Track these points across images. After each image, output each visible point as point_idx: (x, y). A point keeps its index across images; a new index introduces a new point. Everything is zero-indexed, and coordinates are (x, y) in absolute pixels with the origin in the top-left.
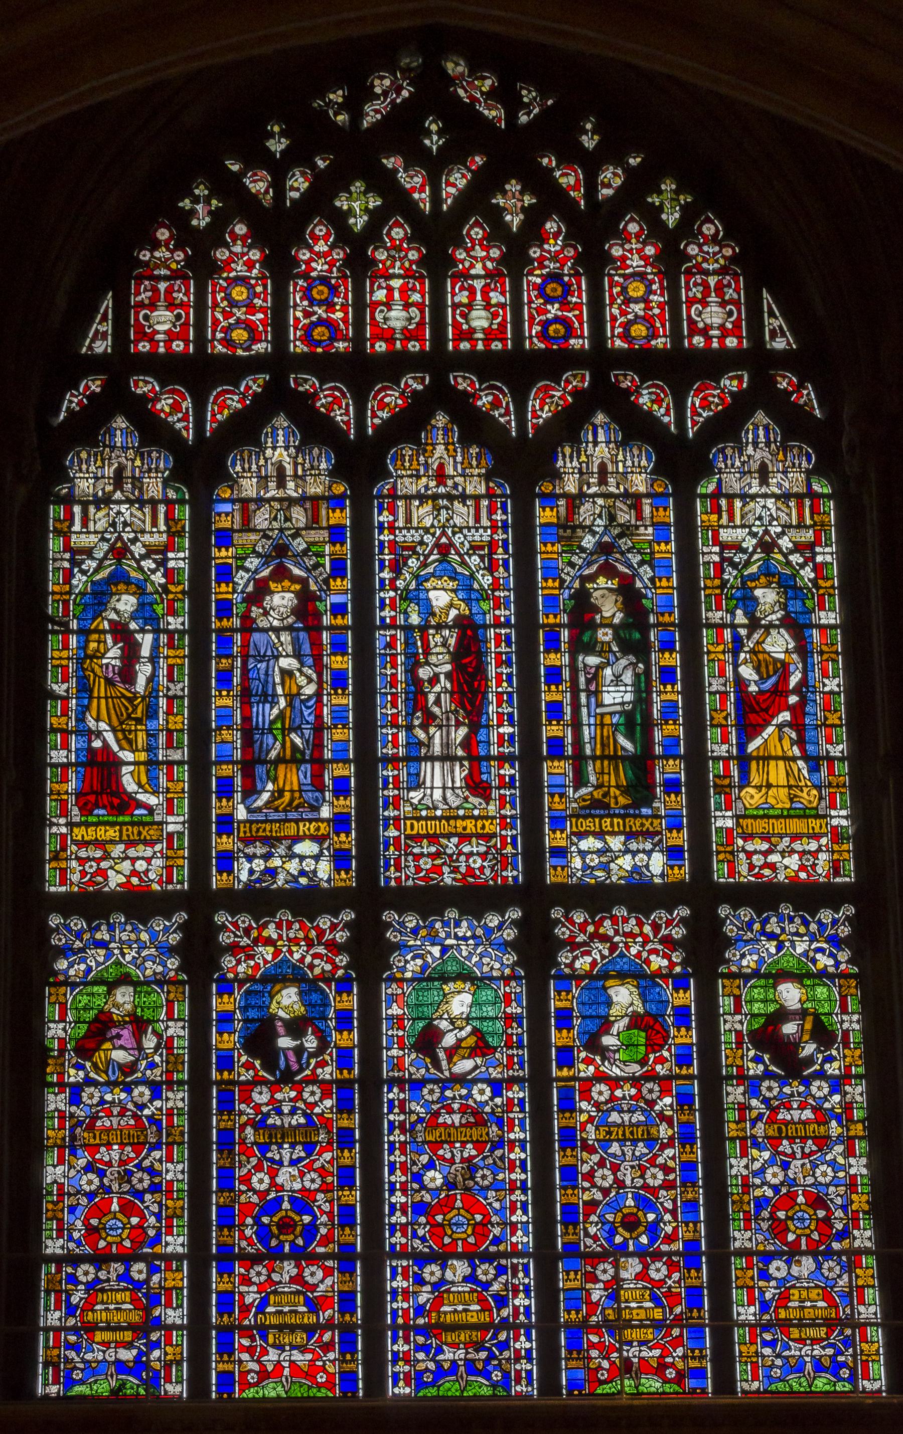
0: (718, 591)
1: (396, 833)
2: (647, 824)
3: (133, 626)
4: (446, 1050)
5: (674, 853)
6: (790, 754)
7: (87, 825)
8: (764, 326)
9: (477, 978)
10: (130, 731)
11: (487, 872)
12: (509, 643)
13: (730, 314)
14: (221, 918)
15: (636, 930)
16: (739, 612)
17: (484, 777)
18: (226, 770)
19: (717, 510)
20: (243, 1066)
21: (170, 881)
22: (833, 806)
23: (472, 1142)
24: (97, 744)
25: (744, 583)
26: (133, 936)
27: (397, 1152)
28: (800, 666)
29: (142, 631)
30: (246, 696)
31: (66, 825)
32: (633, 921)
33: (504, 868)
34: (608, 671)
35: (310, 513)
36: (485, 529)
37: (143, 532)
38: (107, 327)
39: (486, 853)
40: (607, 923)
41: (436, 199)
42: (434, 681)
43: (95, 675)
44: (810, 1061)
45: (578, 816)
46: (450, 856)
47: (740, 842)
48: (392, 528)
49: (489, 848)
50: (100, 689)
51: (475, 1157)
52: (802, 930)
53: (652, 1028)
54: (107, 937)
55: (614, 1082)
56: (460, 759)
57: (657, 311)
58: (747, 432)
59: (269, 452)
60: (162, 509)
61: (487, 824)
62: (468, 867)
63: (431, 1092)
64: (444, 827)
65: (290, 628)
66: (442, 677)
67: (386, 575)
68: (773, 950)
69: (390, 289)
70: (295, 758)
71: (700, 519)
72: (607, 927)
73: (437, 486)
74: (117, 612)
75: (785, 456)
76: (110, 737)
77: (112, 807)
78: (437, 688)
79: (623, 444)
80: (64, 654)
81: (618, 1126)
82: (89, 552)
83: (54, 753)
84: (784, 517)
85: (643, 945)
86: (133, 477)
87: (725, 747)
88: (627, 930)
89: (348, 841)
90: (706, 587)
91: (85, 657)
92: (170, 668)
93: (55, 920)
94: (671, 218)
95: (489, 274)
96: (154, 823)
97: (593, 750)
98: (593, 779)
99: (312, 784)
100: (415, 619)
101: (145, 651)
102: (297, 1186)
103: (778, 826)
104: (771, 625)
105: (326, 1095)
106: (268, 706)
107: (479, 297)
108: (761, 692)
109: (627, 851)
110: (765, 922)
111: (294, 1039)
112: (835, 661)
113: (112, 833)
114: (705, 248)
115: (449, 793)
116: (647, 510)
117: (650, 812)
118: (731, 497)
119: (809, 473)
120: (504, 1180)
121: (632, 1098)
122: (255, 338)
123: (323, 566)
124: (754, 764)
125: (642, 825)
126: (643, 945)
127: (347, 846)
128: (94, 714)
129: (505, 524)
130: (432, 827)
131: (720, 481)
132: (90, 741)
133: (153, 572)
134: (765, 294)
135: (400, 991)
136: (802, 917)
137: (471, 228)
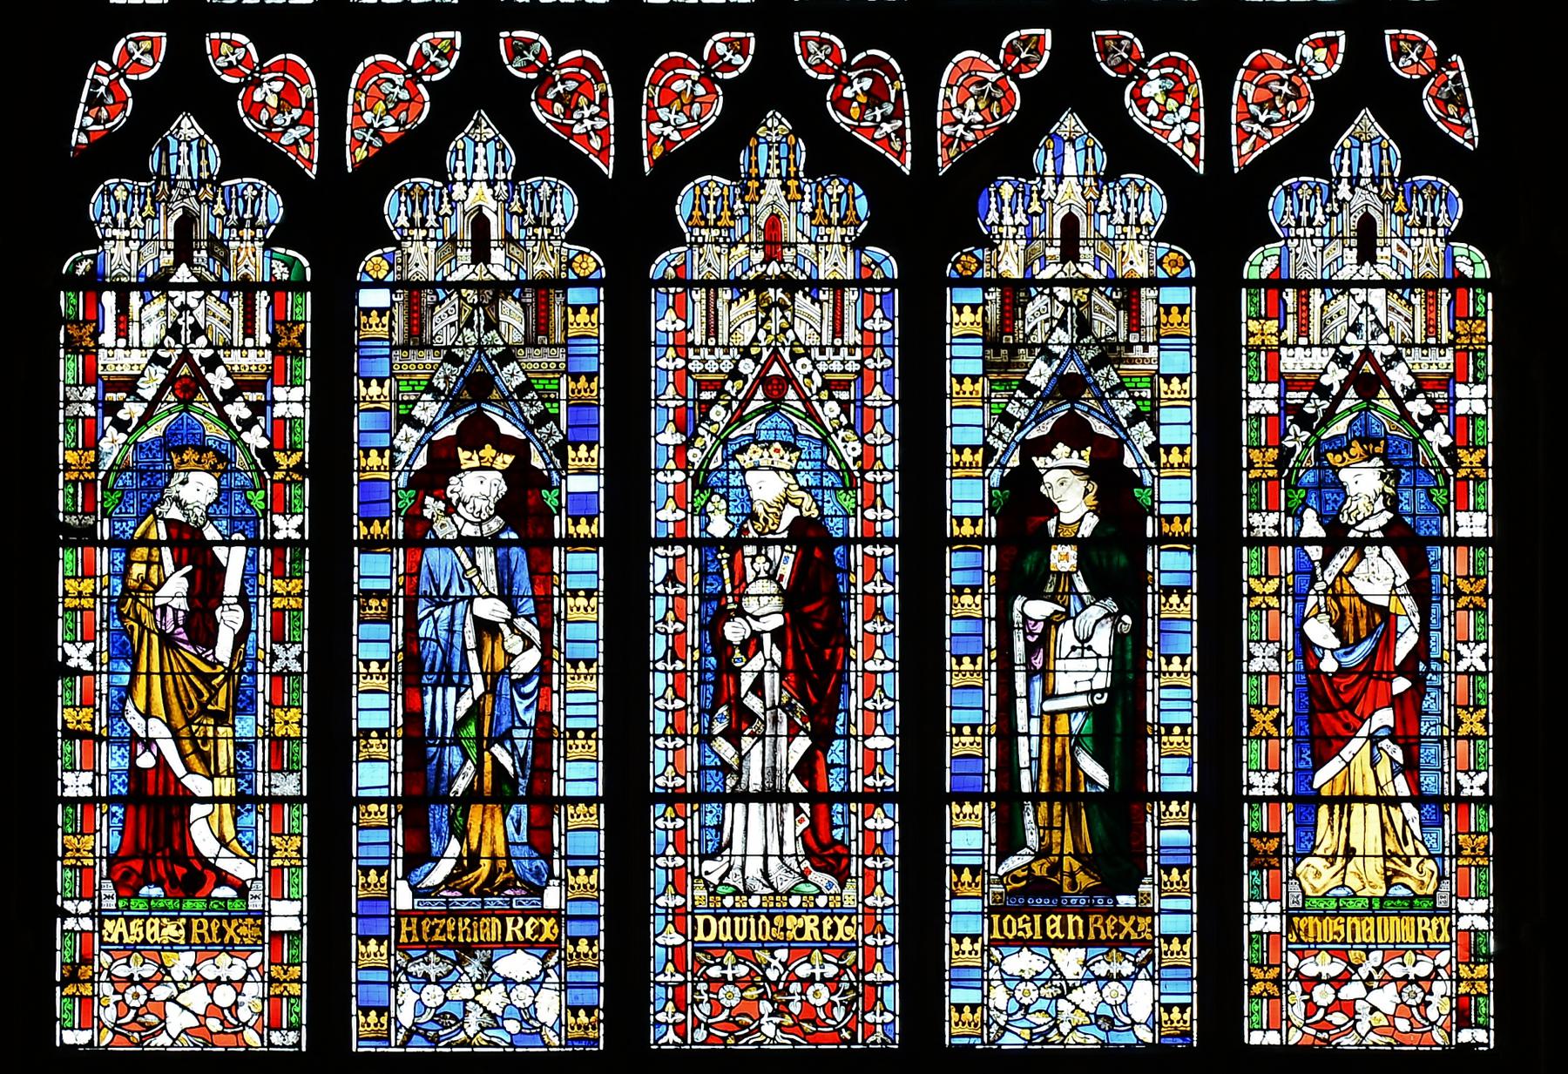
1: (679, 940)
3: (210, 533)
10: (205, 739)
16: (1310, 516)
17: (837, 834)
24: (146, 761)
25: (1320, 456)
28: (1416, 620)
29: (230, 544)
31: (91, 915)
34: (1066, 631)
35: (531, 311)
36: (852, 348)
37: (229, 346)
39: (836, 979)
42: (752, 644)
43: (142, 625)
45: (1002, 911)
47: (1293, 960)
48: (683, 346)
49: (842, 968)
50: (153, 657)
56: (796, 799)
59: (459, 190)
60: (262, 299)
61: (841, 923)
65: (493, 541)
66: (767, 638)
67: (670, 437)
70: (501, 792)
73: (766, 261)
74: (182, 505)
78: (757, 663)
80: (87, 586)
82: (129, 385)
83: (68, 778)
86: (211, 238)
87: (1272, 778)
89: (592, 950)
90: (1251, 464)
92: (278, 614)
96: (249, 913)
97: (1035, 783)
98: (1032, 839)
99: (530, 844)
100: (719, 527)
103: (1363, 929)
106: (452, 691)
108: (1342, 671)
115: (774, 863)
116: (1148, 311)
118: (1303, 286)
123: (556, 419)
124: (1323, 811)
125: (1119, 928)
127: (590, 962)
132: (133, 757)
133: (247, 425)
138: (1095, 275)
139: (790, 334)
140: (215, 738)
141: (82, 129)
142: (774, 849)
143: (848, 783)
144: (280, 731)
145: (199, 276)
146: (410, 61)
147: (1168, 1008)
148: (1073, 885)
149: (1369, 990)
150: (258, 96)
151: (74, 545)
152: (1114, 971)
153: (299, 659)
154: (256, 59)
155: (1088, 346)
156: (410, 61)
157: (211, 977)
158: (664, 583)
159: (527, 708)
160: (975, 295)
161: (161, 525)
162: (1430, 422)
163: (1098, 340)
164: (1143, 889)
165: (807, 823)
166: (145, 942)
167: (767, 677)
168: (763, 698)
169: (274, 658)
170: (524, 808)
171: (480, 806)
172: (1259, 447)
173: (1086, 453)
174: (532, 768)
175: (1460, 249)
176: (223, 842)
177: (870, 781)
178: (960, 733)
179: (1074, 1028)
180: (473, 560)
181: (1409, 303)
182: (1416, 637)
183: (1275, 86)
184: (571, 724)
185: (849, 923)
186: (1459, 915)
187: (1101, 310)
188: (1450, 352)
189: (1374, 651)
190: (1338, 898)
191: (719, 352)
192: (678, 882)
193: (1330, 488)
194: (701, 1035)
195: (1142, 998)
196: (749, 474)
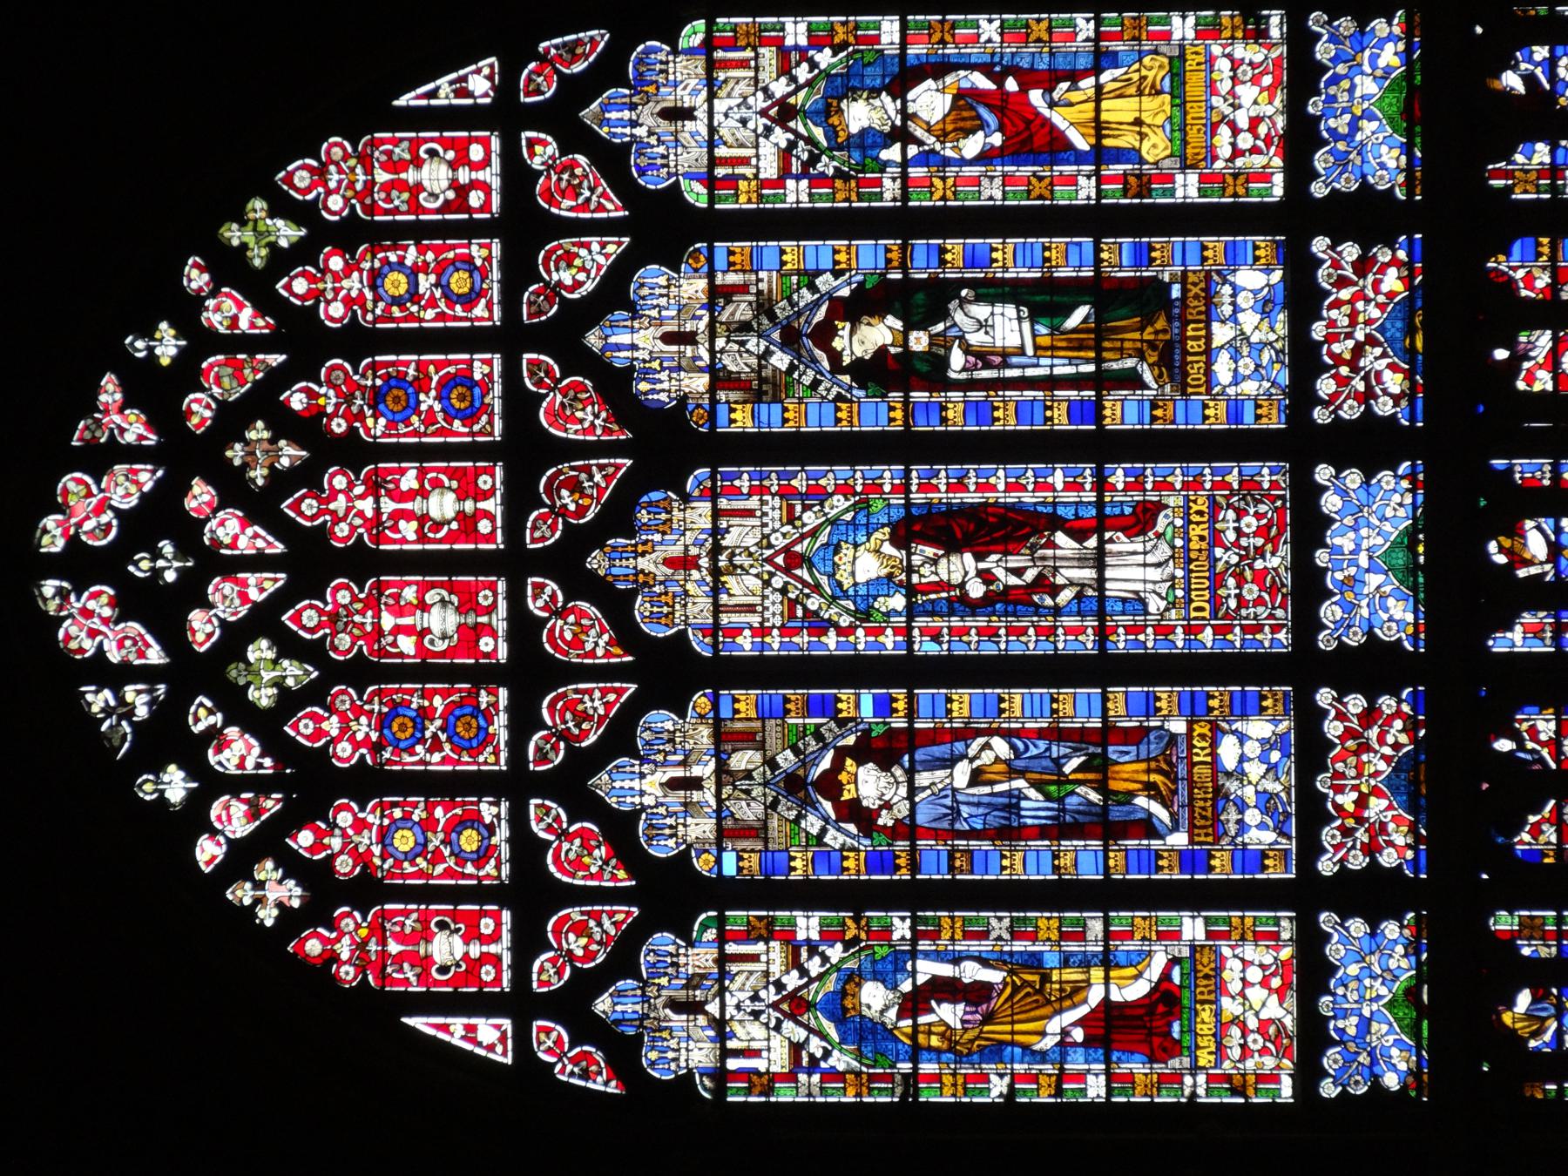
0: (853, 184)
1: (1209, 630)
3: (906, 986)
6: (1091, 92)
8: (451, 107)
10: (1061, 990)
11: (1262, 508)
13: (432, 153)
15: (1346, 309)
16: (885, 155)
17: (1128, 510)
18: (1116, 859)
19: (732, 181)
20: (1535, 838)
22: (1167, 36)
24: (1078, 1035)
25: (840, 148)
26: (1353, 985)
28: (962, 73)
29: (914, 973)
30: (1009, 831)
31: (1194, 1076)
32: (1334, 314)
33: (1259, 485)
35: (739, 745)
36: (763, 503)
37: (767, 974)
38: (458, 1024)
40: (1336, 348)
41: (259, 562)
42: (986, 577)
43: (978, 1038)
44: (1529, 79)
46: (1242, 558)
47: (1219, 164)
48: (762, 631)
49: (1229, 506)
50: (999, 1030)
52: (1345, 84)
54: (1354, 1020)
56: (1102, 542)
57: (430, 256)
58: (615, 135)
59: (649, 801)
60: (731, 948)
61: (1195, 508)
62: (1256, 534)
64: (1200, 565)
65: (911, 773)
66: (982, 565)
67: (831, 639)
68: (1374, 125)
69: (397, 630)
70: (1099, 768)
71: (743, 204)
72: (1343, 348)
73: (699, 568)
74: (886, 1008)
75: (652, 83)
78: (1000, 573)
80: (948, 1080)
82: (796, 1048)
83: (1092, 1093)
84: (742, 88)
86: (686, 987)
87: (1082, 181)
88: (1346, 321)
89: (1218, 695)
90: (847, 200)
92: (968, 935)
93: (1328, 1090)
94: (287, 233)
95: (374, 489)
96: (1192, 956)
97: (1088, 361)
98: (1130, 363)
99: (1137, 744)
100: (898, 602)
103: (1195, 111)
104: (903, 112)
106: (1024, 804)
107: (408, 506)
108: (1001, 129)
109: (1234, 318)
112: (954, 25)
113: (1206, 1014)
114: (332, 185)
115: (1150, 559)
116: (733, 278)
118: (713, 162)
119: (675, 51)
122: (473, 820)
123: (818, 726)
124: (1107, 142)
125: (1196, 297)
126: (1368, 301)
127: (1227, 698)
128: (1034, 1039)
130: (1201, 583)
131: (690, 176)
132: (1075, 1044)
133: (825, 959)
134: (402, 102)
136: (1329, 83)
137: (301, 514)
138: (706, 319)
139: (753, 550)
140: (1061, 982)
141: (606, 1084)
142: (1140, 559)
143: (1089, 503)
144: (1054, 935)
145: (714, 996)
146: (552, 838)
147: (1256, 259)
148: (1164, 331)
150: (580, 953)
151: (917, 1090)
152: (1229, 300)
153: (1000, 919)
154: (551, 954)
155: (759, 324)
156: (552, 838)
157: (1240, 985)
158: (940, 643)
160: (722, 410)
161: (902, 1024)
162: (813, 65)
163: (755, 317)
164: (1167, 279)
165: (1120, 534)
166: (1214, 1035)
167: (1010, 565)
168: (1025, 568)
169: (999, 938)
170: (1111, 749)
172: (834, 194)
173: (840, 325)
174: (1081, 742)
175: (683, 43)
176: (1139, 976)
177: (1088, 487)
178: (1051, 419)
179: (1272, 329)
180: (924, 789)
181: (726, 81)
182: (976, 74)
183: (563, 184)
184: (1047, 712)
185: (1195, 502)
186: (1183, 39)
187: (733, 314)
188: (762, 50)
190: (1172, 131)
191: (767, 603)
192: (1164, 630)
194: (1280, 613)
195: (1251, 279)
196: (859, 579)
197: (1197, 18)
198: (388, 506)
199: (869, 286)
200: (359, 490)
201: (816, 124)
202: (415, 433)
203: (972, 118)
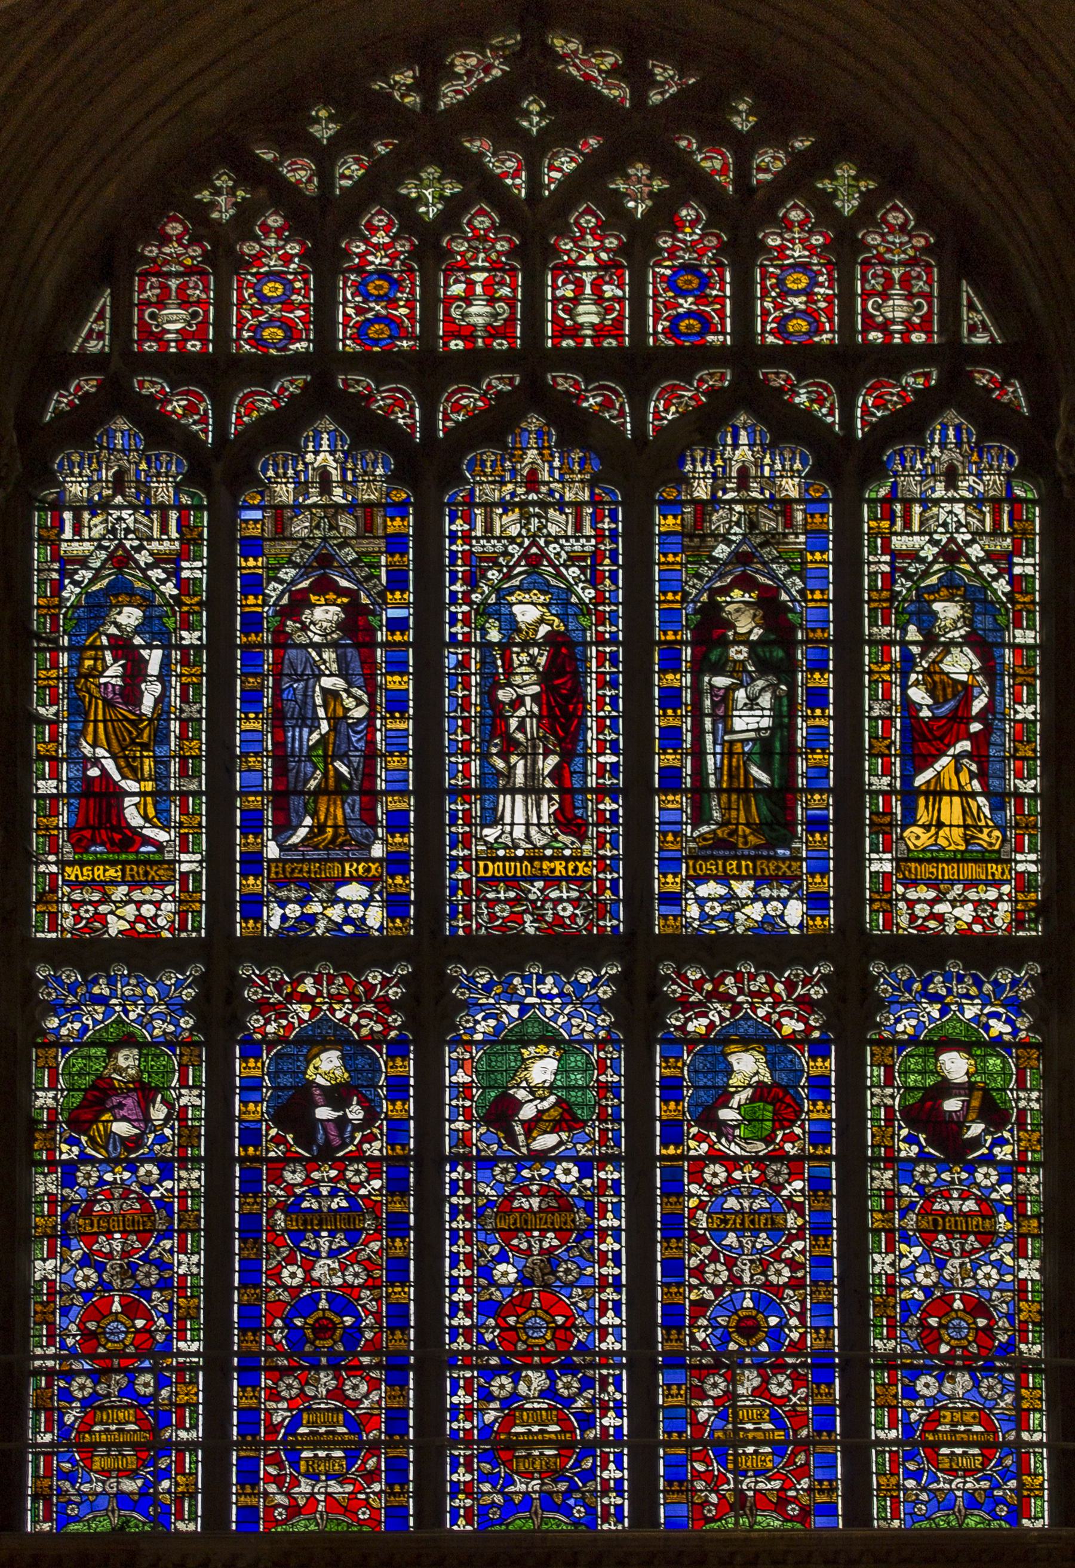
1: (466, 876)
2: (784, 867)
4: (523, 1123)
5: (816, 901)
6: (968, 789)
7: (82, 864)
9: (564, 1041)
10: (135, 758)
12: (614, 662)
14: (246, 971)
17: (579, 812)
21: (183, 927)
23: (554, 1230)
24: (94, 772)
27: (461, 1242)
28: (986, 689)
31: (56, 863)
32: (762, 979)
34: (741, 694)
39: (578, 899)
40: (730, 980)
42: (518, 702)
43: (91, 696)
45: (696, 858)
46: (533, 902)
47: (900, 889)
51: (558, 1247)
53: (781, 1101)
55: (732, 1162)
56: (549, 792)
62: (556, 915)
63: (505, 1171)
66: (528, 700)
76: (110, 765)
77: (112, 842)
78: (522, 712)
79: (771, 447)
81: (736, 1213)
83: (41, 784)
85: (774, 1005)
87: (886, 780)
89: (406, 883)
91: (78, 677)
92: (184, 687)
97: (718, 782)
98: (716, 815)
101: (153, 669)
102: (337, 1281)
105: (372, 1175)
106: (306, 731)
109: (757, 898)
110: (929, 980)
111: (334, 1110)
112: (1031, 686)
115: (533, 831)
117: (788, 853)
120: (592, 1275)
121: (753, 1180)
124: (922, 801)
125: (778, 868)
126: (774, 1005)
127: (404, 890)
128: (90, 739)
129: (614, 533)
132: (85, 769)
135: (467, 1056)
143: (586, 782)
148: (746, 843)
149: (954, 907)
152: (775, 894)
159: (359, 740)
165: (556, 806)
166: (93, 880)
168: (525, 733)
170: (357, 798)
171: (325, 798)
174: (363, 774)
176: (146, 818)
178: (665, 753)
185: (586, 865)
189: (955, 710)
190: (932, 851)
193: (926, 619)
197: (1035, 874)
198: (588, 278)
199: (790, 616)
200: (604, 256)
201: (939, 579)
202: (656, 294)
203: (945, 695)
